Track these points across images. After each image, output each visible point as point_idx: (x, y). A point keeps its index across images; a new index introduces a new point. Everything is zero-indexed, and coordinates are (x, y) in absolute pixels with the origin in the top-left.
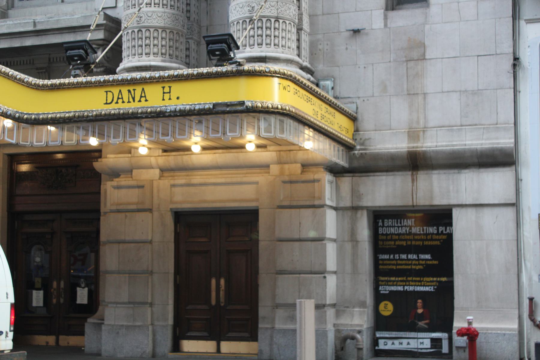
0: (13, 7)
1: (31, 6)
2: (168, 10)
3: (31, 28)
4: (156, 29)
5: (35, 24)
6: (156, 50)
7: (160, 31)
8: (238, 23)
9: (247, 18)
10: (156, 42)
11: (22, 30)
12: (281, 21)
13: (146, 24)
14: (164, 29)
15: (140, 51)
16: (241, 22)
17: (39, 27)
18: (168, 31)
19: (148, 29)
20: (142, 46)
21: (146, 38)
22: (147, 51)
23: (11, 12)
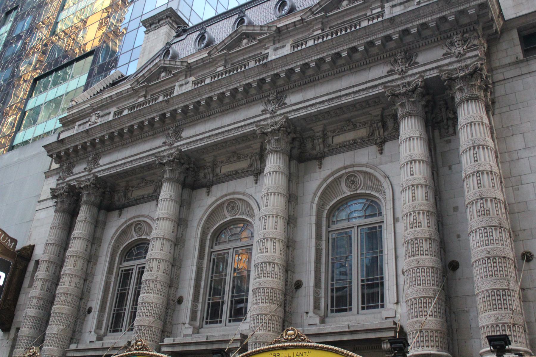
0: (327, 316)
1: (338, 316)
2: (438, 319)
3: (347, 330)
4: (432, 331)
5: (349, 327)
6: (432, 344)
7: (434, 332)
8: (488, 327)
9: (495, 324)
10: (432, 339)
11: (342, 330)
12: (516, 326)
13: (426, 328)
14: (436, 331)
15: (422, 345)
16: (490, 326)
17: (352, 329)
18: (439, 332)
19: (427, 331)
20: (423, 341)
21: (426, 336)
22: (427, 344)
23: (327, 320)
